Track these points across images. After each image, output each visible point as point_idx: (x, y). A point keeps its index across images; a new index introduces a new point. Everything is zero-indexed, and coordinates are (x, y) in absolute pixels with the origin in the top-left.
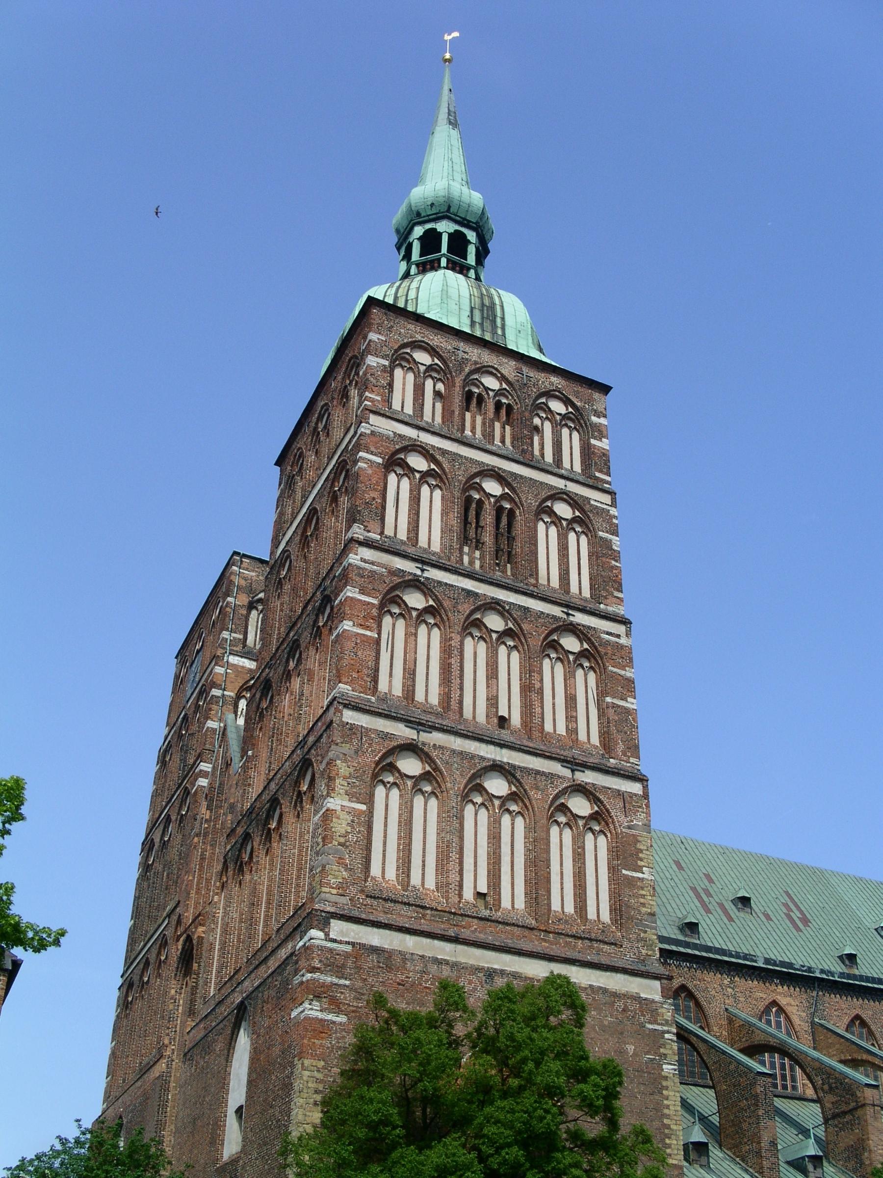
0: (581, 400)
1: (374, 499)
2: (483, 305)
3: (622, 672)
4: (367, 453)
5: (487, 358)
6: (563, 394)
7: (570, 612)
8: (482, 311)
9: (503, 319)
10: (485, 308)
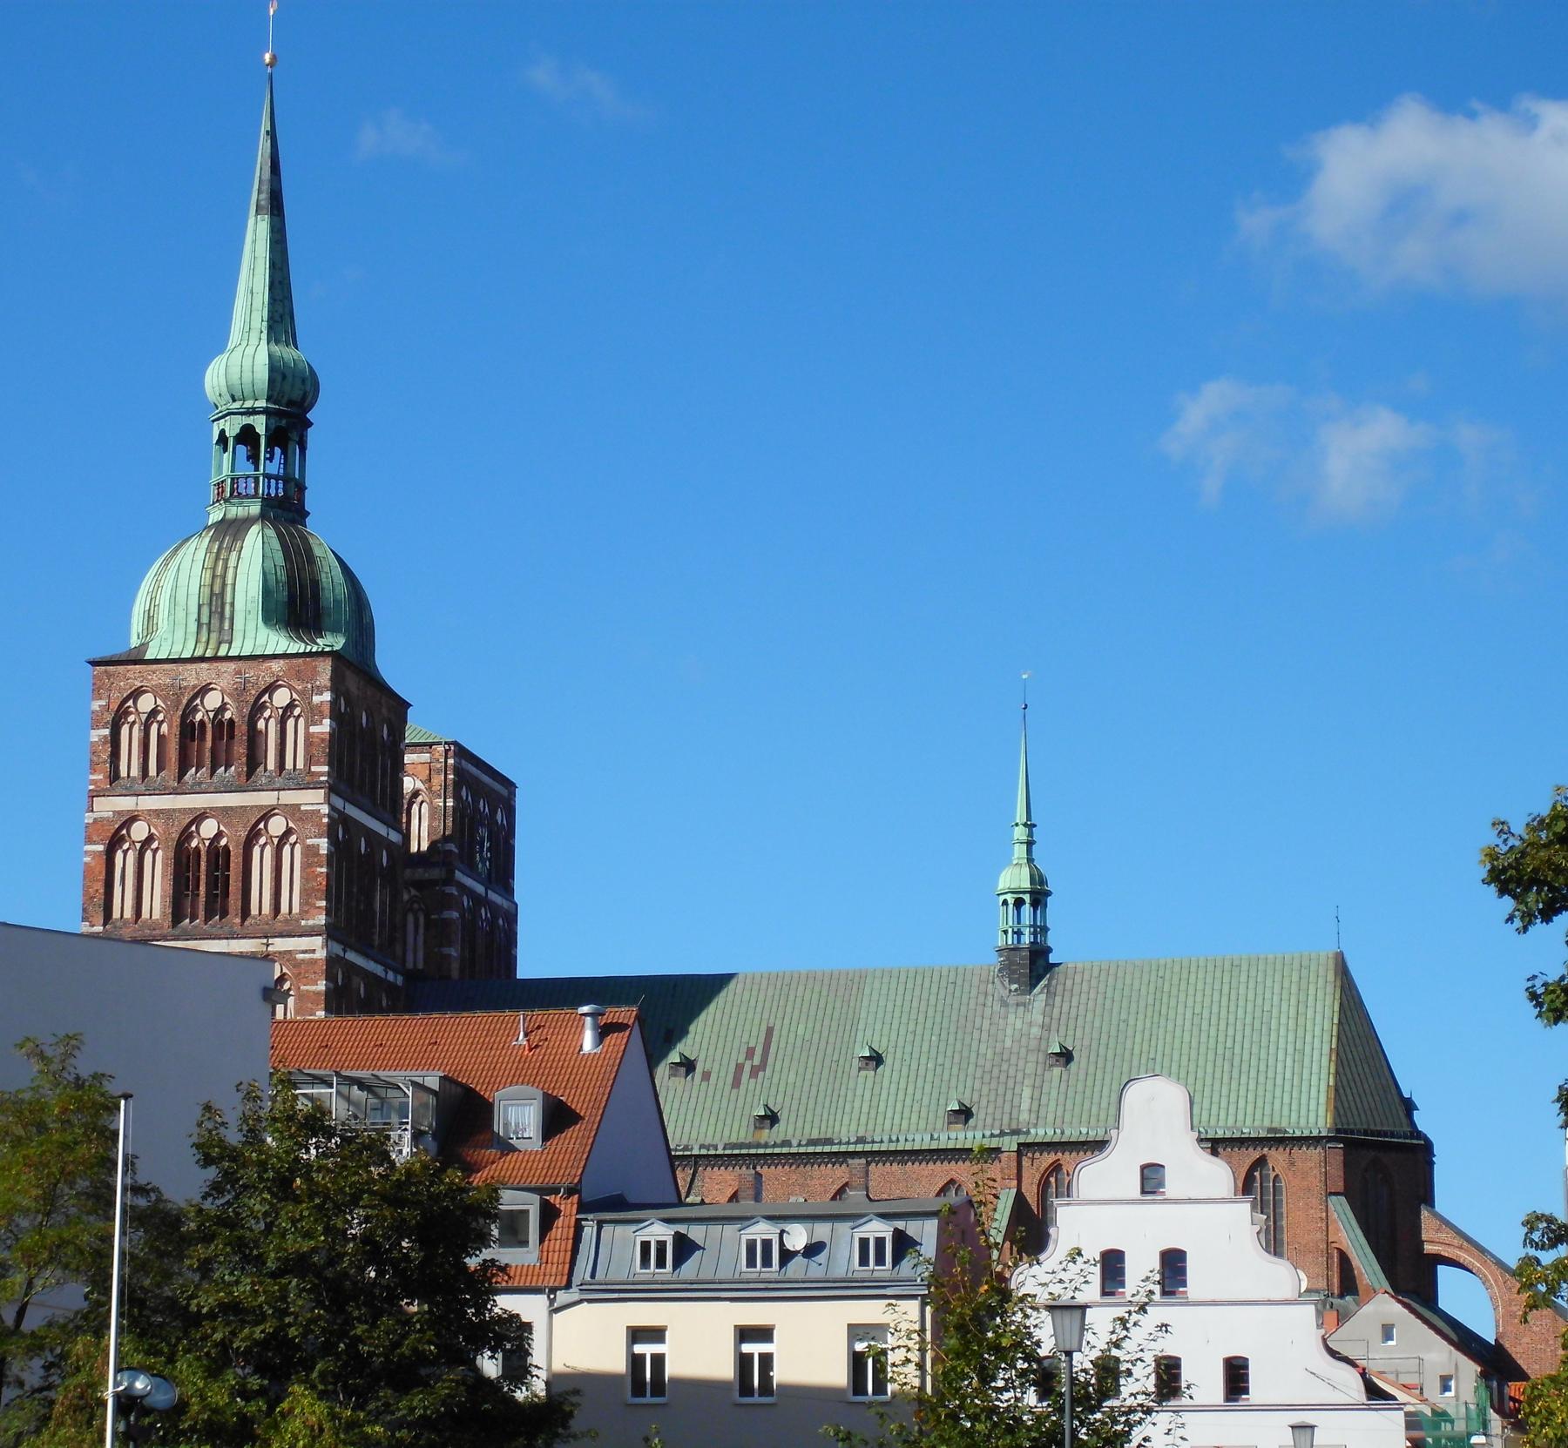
1: (97, 890)
2: (212, 593)
3: (313, 988)
5: (204, 672)
8: (210, 604)
9: (232, 604)
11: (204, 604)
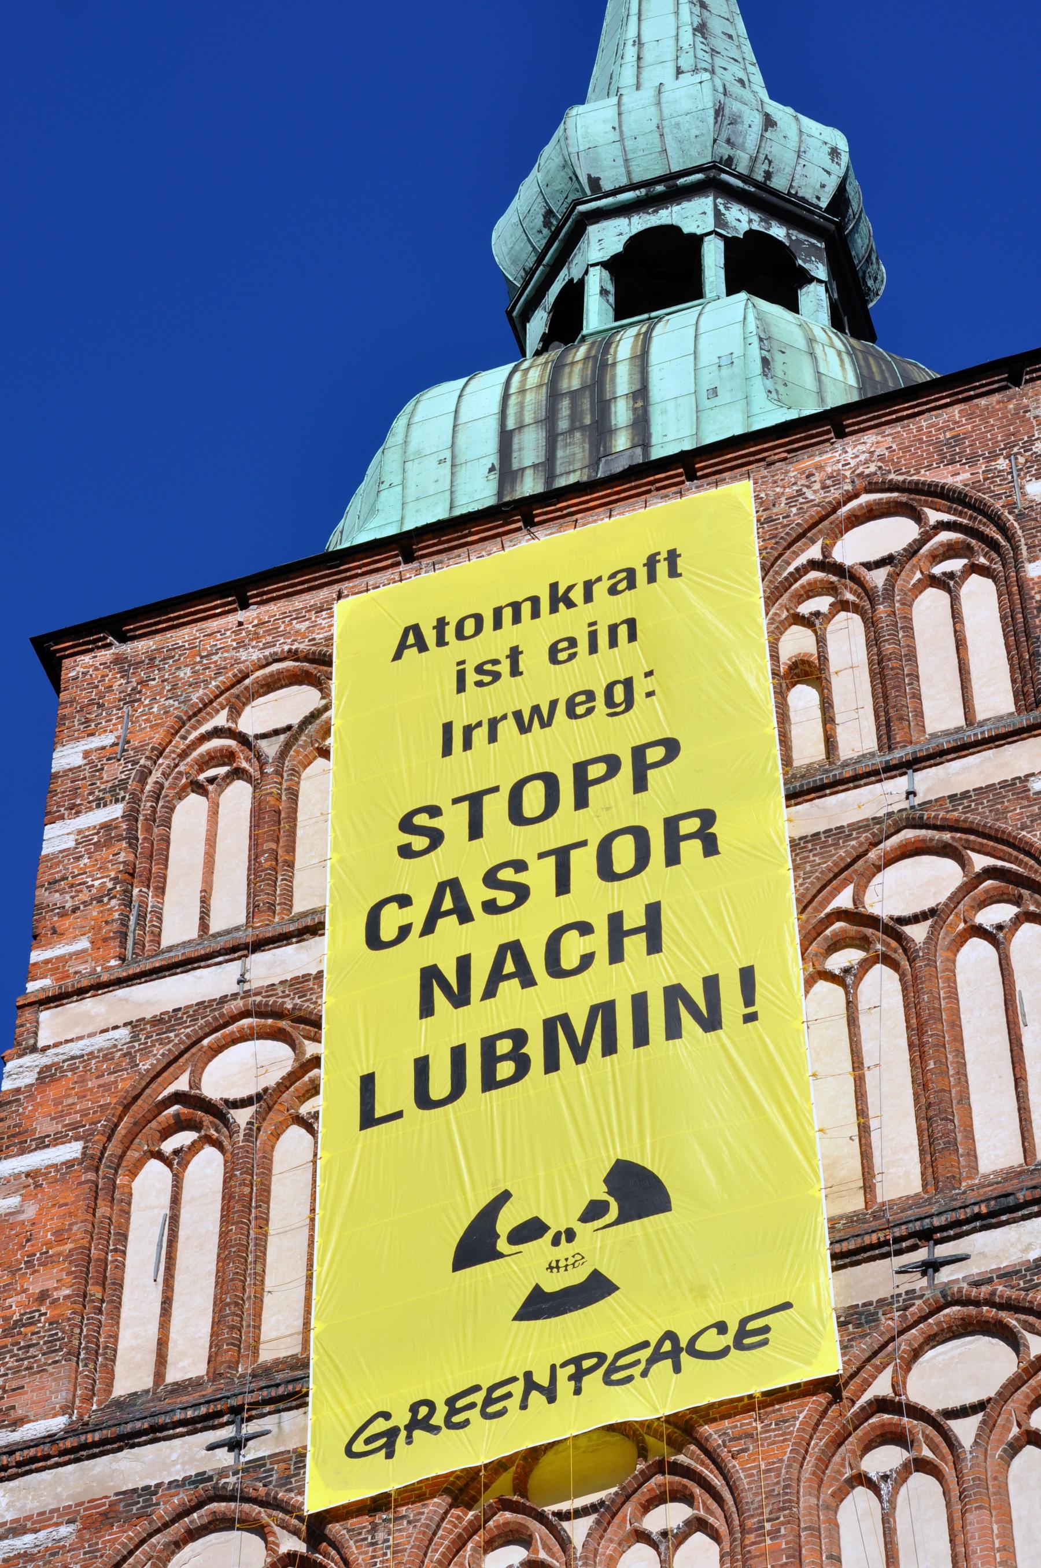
0: (972, 460)
1: (43, 1296)
4: (22, 1152)
6: (893, 487)
7: (943, 1251)
8: (550, 419)
9: (641, 394)
10: (565, 404)
11: (521, 427)
